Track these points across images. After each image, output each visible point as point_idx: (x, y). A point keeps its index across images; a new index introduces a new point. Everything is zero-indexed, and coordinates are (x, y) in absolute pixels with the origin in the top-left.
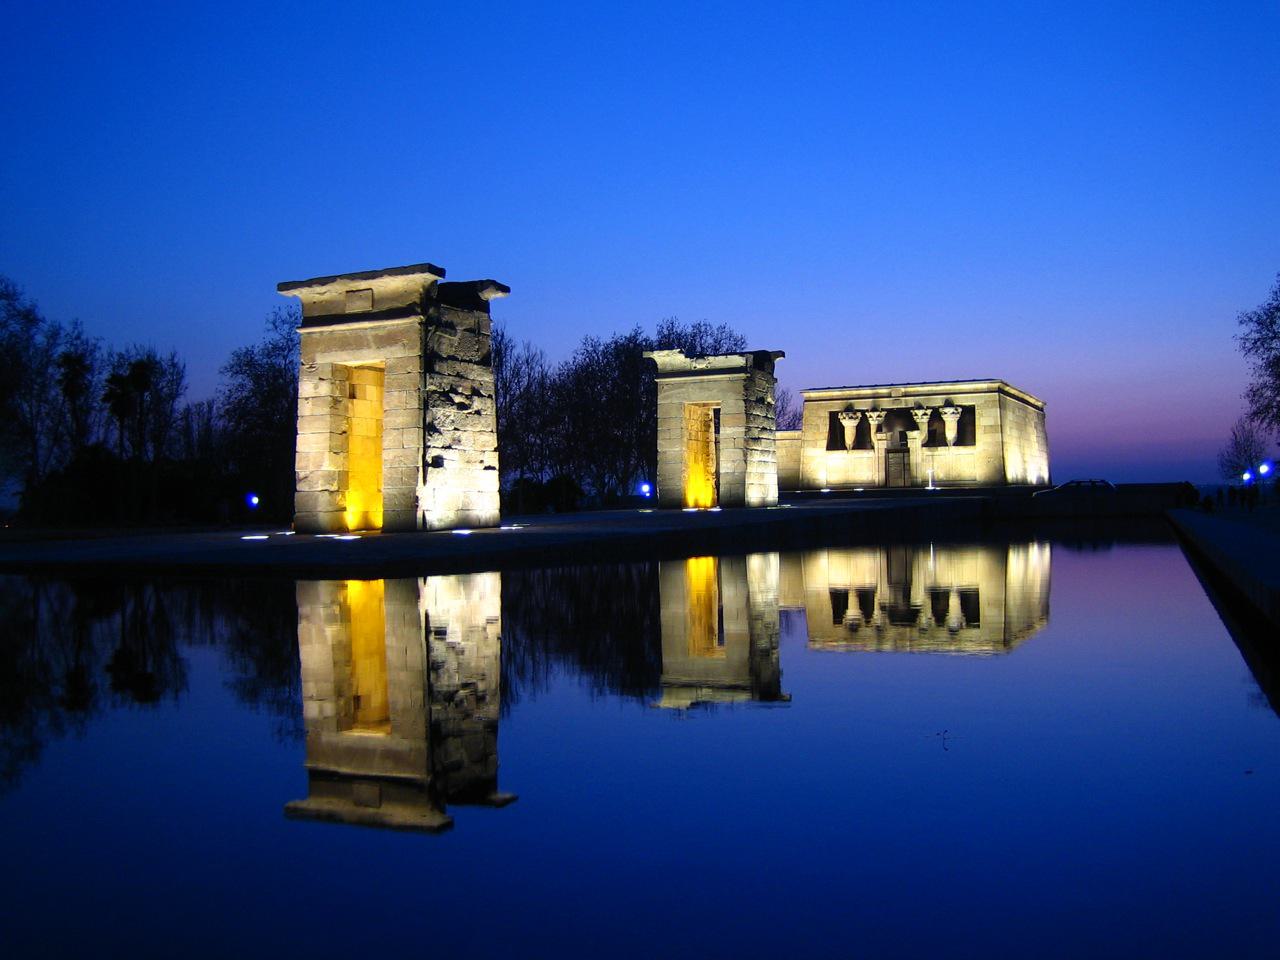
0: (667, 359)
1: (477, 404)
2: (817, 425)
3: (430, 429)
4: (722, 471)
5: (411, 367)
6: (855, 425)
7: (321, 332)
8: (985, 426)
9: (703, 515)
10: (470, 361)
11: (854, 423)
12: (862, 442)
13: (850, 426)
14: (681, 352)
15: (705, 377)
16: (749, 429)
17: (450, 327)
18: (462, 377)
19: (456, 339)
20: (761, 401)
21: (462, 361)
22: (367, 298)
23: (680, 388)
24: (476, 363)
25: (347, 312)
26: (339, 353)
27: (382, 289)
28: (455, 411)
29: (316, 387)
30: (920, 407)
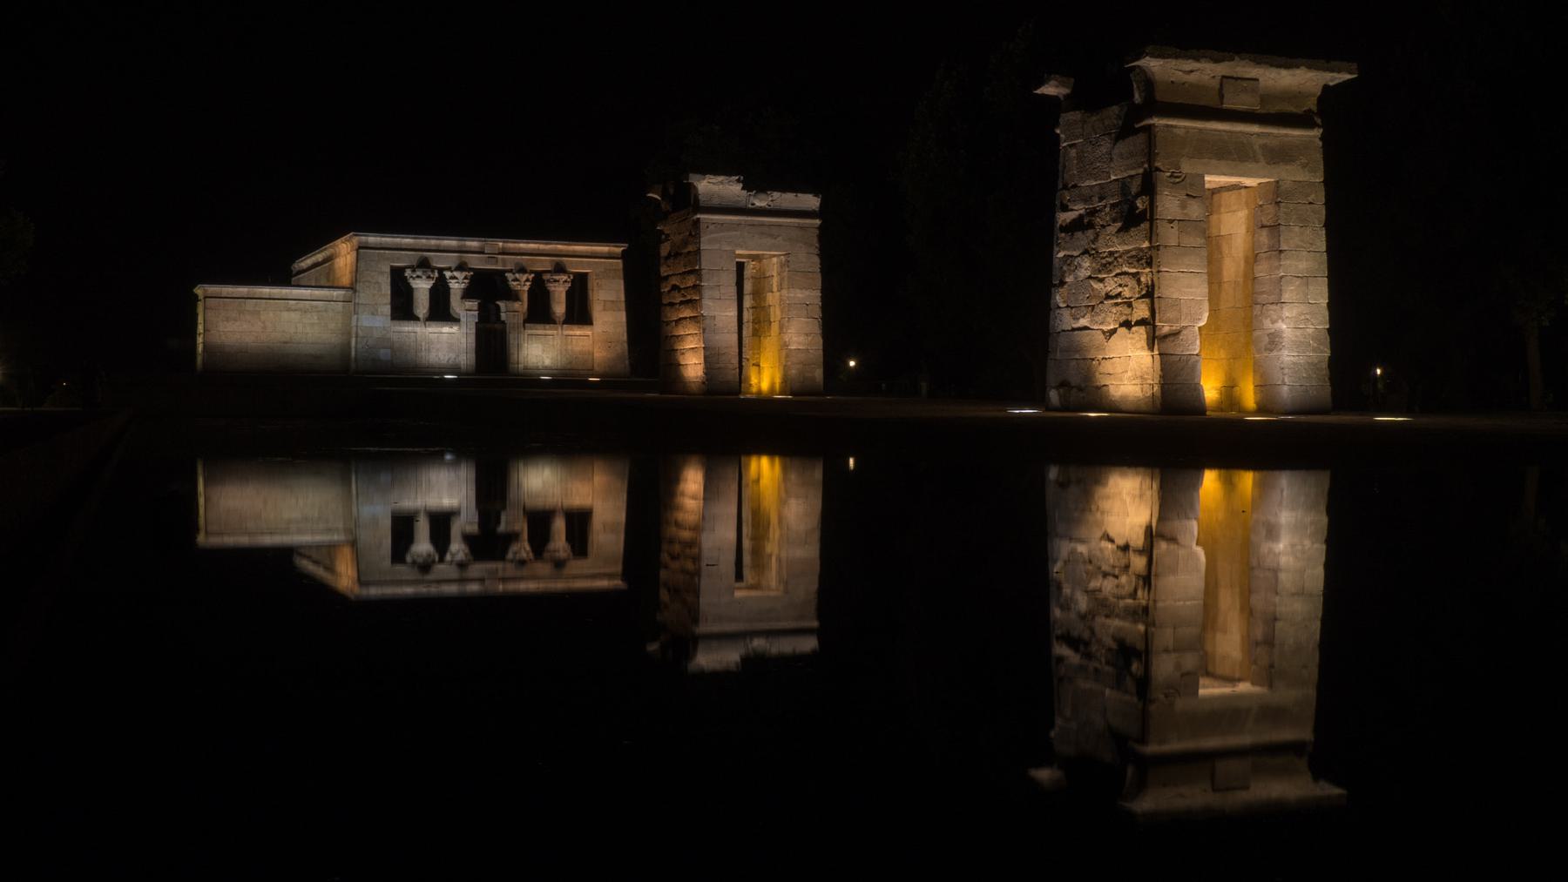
0: (716, 188)
2: (378, 283)
5: (1313, 196)
6: (429, 287)
7: (1185, 127)
12: (440, 311)
13: (422, 286)
14: (738, 181)
26: (1214, 162)
27: (1271, 83)
29: (1183, 206)
30: (523, 270)
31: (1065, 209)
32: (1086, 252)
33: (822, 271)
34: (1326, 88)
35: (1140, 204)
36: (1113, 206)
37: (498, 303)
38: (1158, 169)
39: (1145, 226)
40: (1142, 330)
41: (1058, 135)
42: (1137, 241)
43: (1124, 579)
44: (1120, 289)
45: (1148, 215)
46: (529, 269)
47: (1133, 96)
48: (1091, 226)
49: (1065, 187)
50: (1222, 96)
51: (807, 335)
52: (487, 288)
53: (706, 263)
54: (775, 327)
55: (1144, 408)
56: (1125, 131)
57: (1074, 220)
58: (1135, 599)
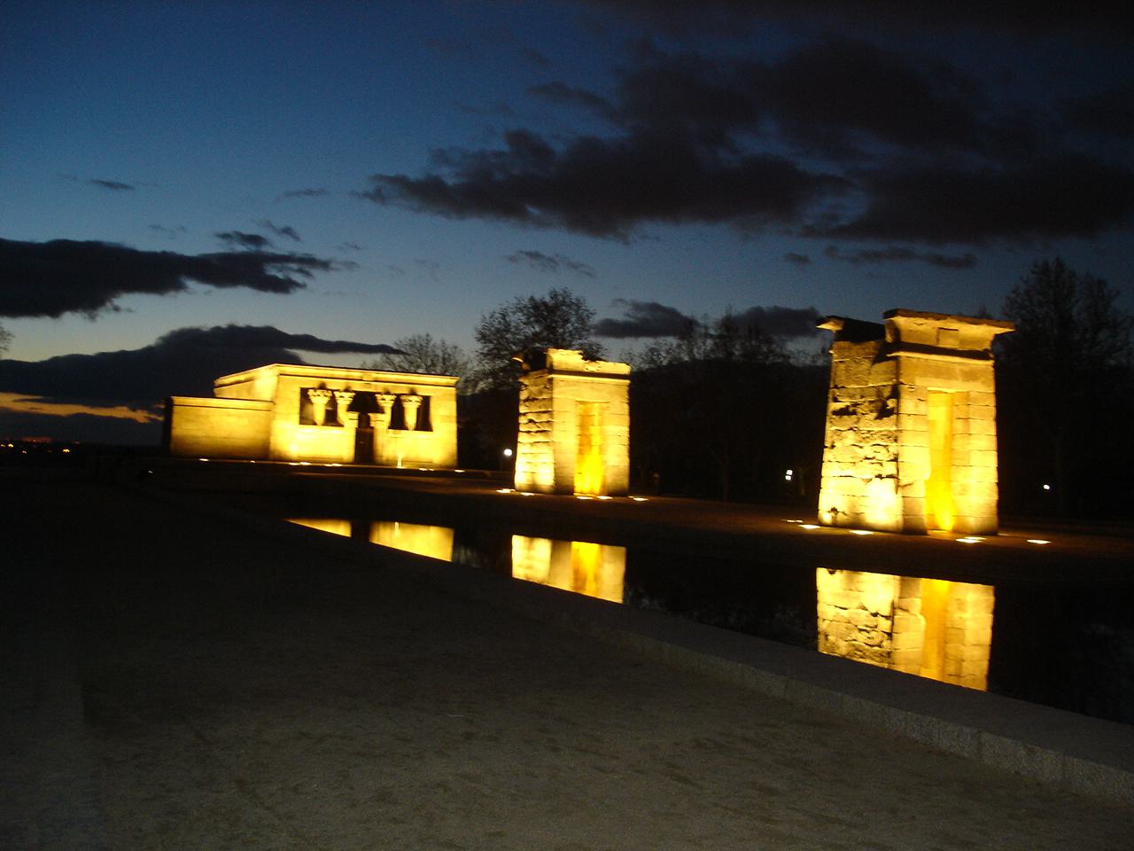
7: (919, 358)
8: (442, 416)
11: (326, 400)
12: (331, 418)
13: (319, 403)
14: (580, 354)
23: (575, 385)
25: (941, 346)
26: (934, 380)
29: (916, 406)
30: (388, 393)
31: (836, 400)
32: (851, 429)
33: (631, 414)
34: (997, 336)
35: (891, 404)
36: (871, 402)
37: (371, 415)
39: (894, 417)
40: (892, 480)
41: (831, 354)
42: (888, 425)
43: (873, 634)
44: (875, 454)
45: (895, 411)
46: (392, 392)
47: (884, 336)
48: (854, 413)
49: (836, 387)
50: (938, 340)
51: (619, 456)
52: (364, 404)
53: (556, 406)
54: (595, 450)
55: (890, 529)
56: (879, 358)
57: (842, 409)
58: (880, 646)
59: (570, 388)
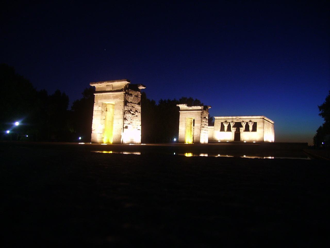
1: (137, 114)
2: (218, 125)
3: (125, 119)
4: (195, 134)
7: (100, 95)
8: (259, 127)
9: (189, 145)
10: (135, 103)
11: (227, 125)
12: (229, 130)
13: (226, 126)
14: (186, 105)
15: (192, 111)
16: (202, 124)
17: (131, 95)
18: (133, 107)
19: (132, 98)
20: (205, 118)
21: (134, 103)
22: (111, 87)
24: (137, 104)
27: (115, 85)
28: (131, 115)
29: (98, 108)
30: (243, 122)
37: (240, 128)
38: (95, 102)
46: (245, 122)
52: (238, 125)
59: (184, 114)
